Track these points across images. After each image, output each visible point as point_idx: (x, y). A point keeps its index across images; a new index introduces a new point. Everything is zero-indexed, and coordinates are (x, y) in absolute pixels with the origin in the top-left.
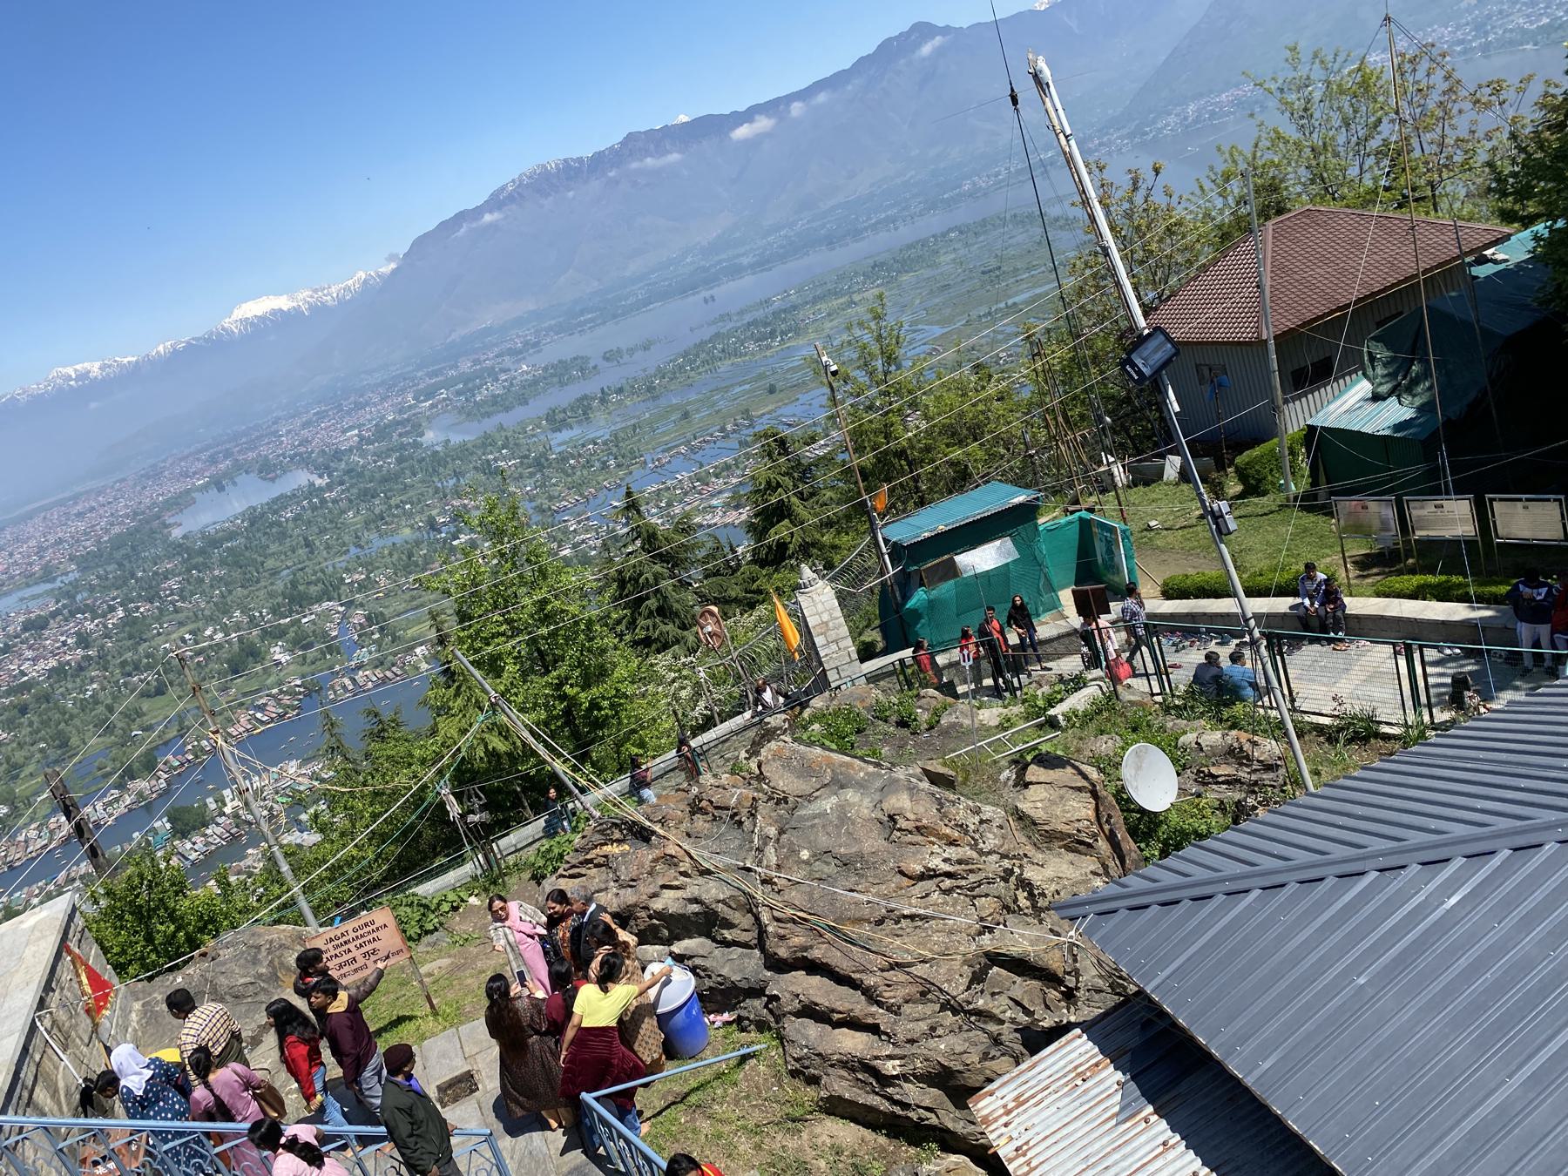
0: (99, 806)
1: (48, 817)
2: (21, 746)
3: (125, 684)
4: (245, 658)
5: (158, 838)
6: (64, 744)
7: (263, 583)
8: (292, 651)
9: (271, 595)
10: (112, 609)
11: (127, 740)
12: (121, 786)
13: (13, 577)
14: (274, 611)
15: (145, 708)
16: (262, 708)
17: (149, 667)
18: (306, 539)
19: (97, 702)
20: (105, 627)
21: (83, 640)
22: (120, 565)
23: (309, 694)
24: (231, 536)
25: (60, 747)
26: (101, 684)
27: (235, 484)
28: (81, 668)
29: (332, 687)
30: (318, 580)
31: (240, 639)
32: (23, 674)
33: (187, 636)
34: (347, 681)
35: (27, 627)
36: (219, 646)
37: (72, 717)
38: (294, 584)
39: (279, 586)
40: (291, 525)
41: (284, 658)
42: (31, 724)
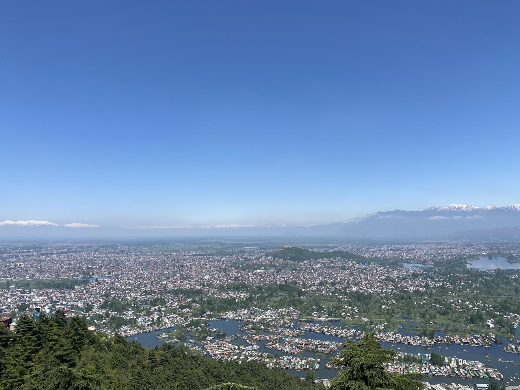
0: (412, 338)
1: (397, 333)
2: (398, 308)
3: (434, 306)
4: (476, 319)
5: (425, 360)
6: (409, 314)
7: (493, 296)
8: (495, 325)
9: (495, 302)
10: (439, 281)
11: (427, 323)
12: (421, 337)
13: (414, 259)
14: (494, 307)
15: (437, 316)
16: (477, 338)
17: (443, 304)
18: (516, 288)
19: (423, 307)
20: (435, 285)
21: (427, 286)
22: (447, 269)
23: (496, 343)
24: (488, 275)
25: (408, 314)
26: (427, 302)
27: (496, 259)
28: (423, 294)
29: (507, 346)
30: (516, 305)
31: (478, 311)
32: (406, 288)
33: (460, 301)
34: (513, 347)
35: (413, 275)
36: (469, 309)
37: (415, 307)
38: (506, 302)
39: (499, 300)
40: (512, 281)
41: (492, 326)
42: (403, 303)
